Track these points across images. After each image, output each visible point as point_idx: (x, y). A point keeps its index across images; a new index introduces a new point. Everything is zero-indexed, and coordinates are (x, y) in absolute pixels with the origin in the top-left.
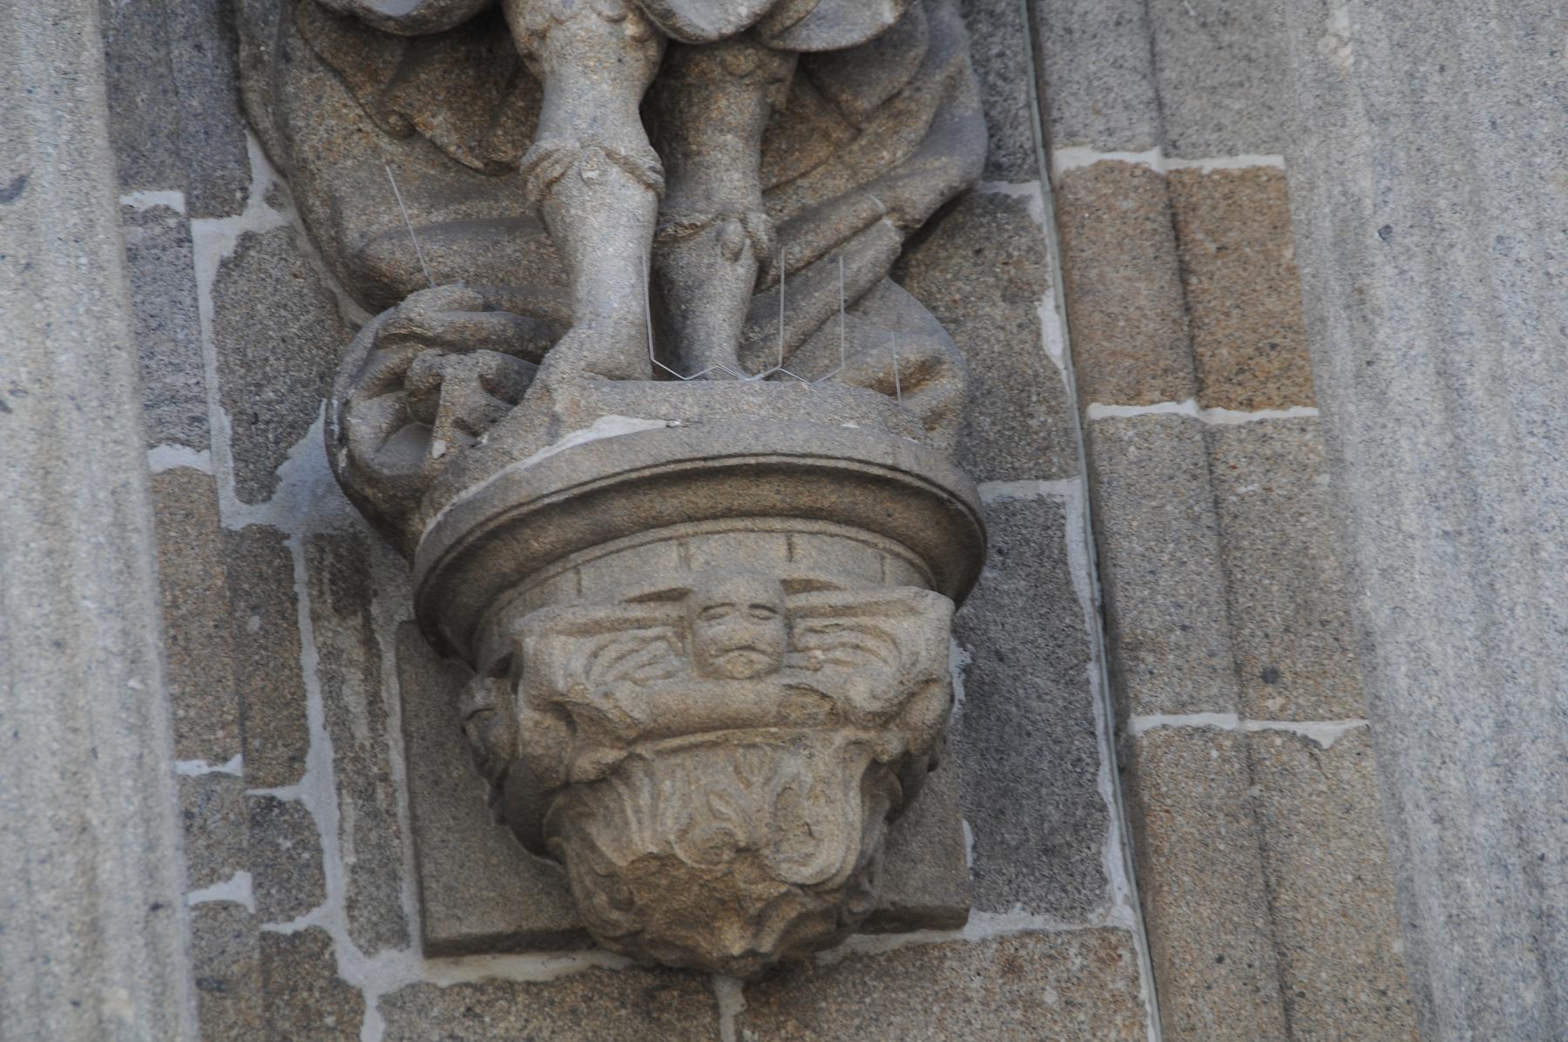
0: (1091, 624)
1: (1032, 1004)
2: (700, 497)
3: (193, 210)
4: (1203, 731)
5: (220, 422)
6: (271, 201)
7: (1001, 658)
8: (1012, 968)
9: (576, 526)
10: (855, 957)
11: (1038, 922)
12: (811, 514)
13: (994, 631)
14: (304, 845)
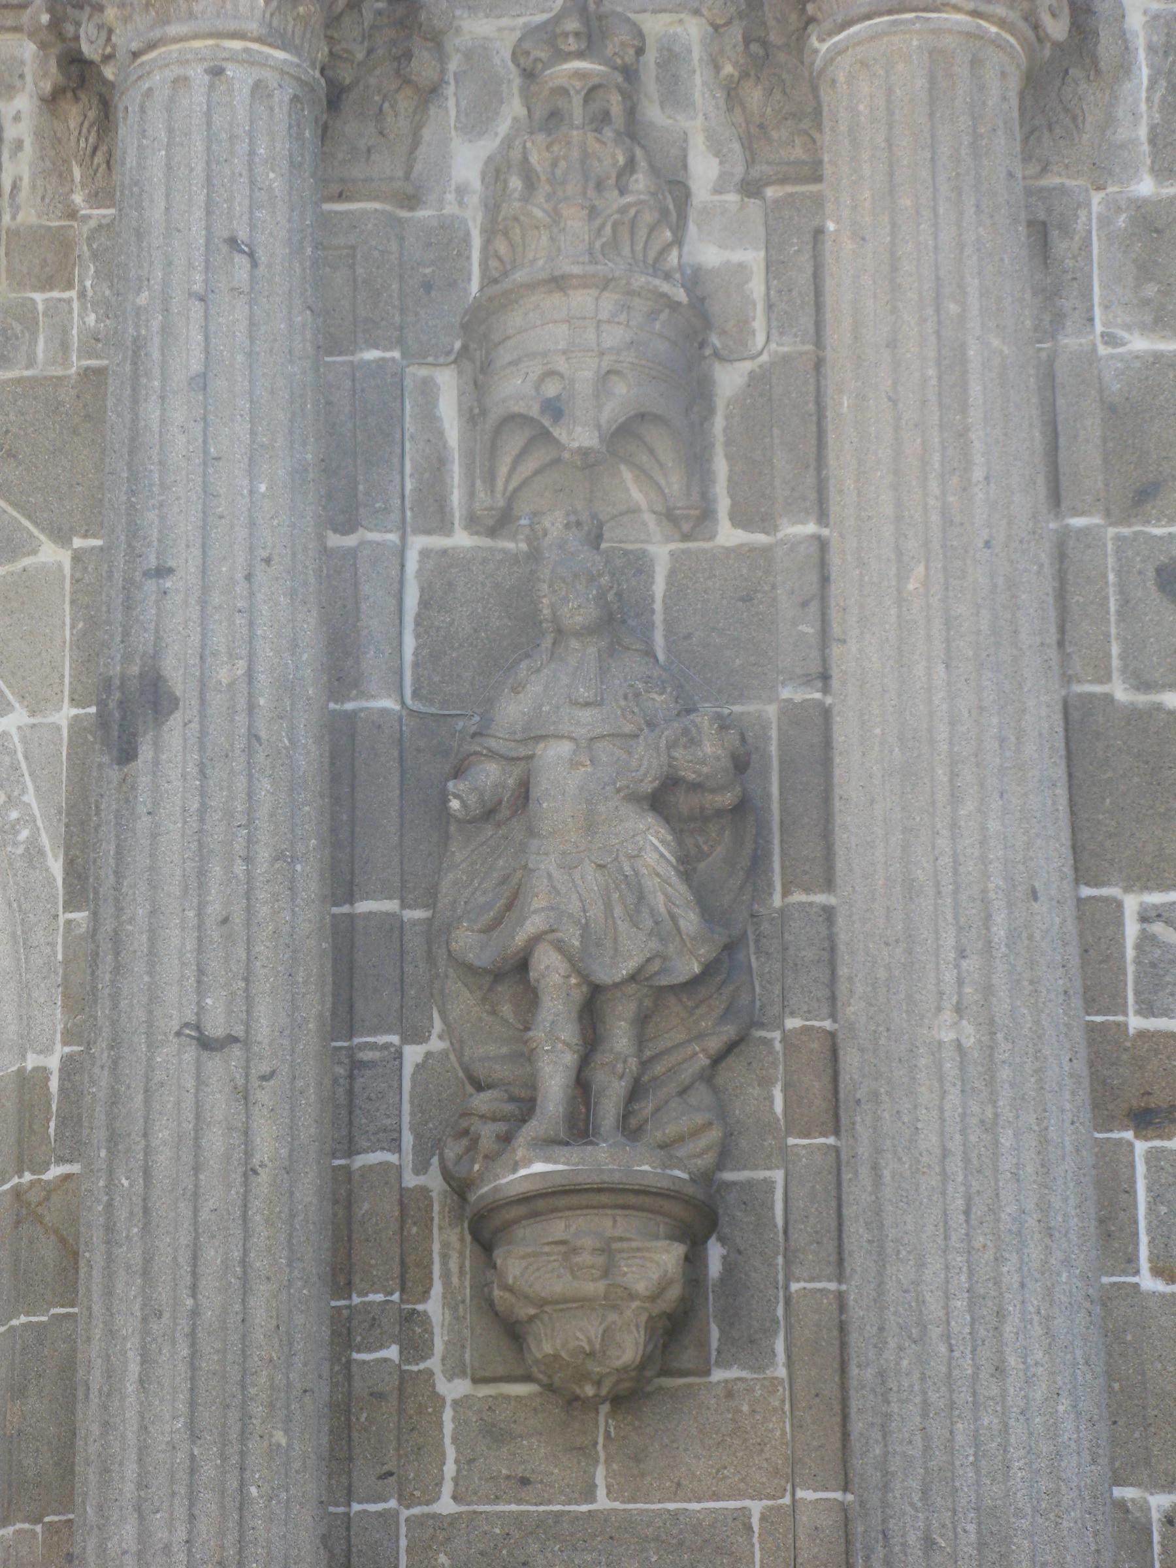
0: (781, 1237)
1: (738, 1411)
2: (574, 1200)
3: (406, 1040)
4: (821, 1290)
5: (408, 1139)
6: (440, 1037)
7: (740, 1252)
8: (730, 1395)
9: (522, 1210)
10: (660, 1388)
11: (744, 1374)
12: (624, 1207)
13: (738, 1240)
14: (426, 1331)
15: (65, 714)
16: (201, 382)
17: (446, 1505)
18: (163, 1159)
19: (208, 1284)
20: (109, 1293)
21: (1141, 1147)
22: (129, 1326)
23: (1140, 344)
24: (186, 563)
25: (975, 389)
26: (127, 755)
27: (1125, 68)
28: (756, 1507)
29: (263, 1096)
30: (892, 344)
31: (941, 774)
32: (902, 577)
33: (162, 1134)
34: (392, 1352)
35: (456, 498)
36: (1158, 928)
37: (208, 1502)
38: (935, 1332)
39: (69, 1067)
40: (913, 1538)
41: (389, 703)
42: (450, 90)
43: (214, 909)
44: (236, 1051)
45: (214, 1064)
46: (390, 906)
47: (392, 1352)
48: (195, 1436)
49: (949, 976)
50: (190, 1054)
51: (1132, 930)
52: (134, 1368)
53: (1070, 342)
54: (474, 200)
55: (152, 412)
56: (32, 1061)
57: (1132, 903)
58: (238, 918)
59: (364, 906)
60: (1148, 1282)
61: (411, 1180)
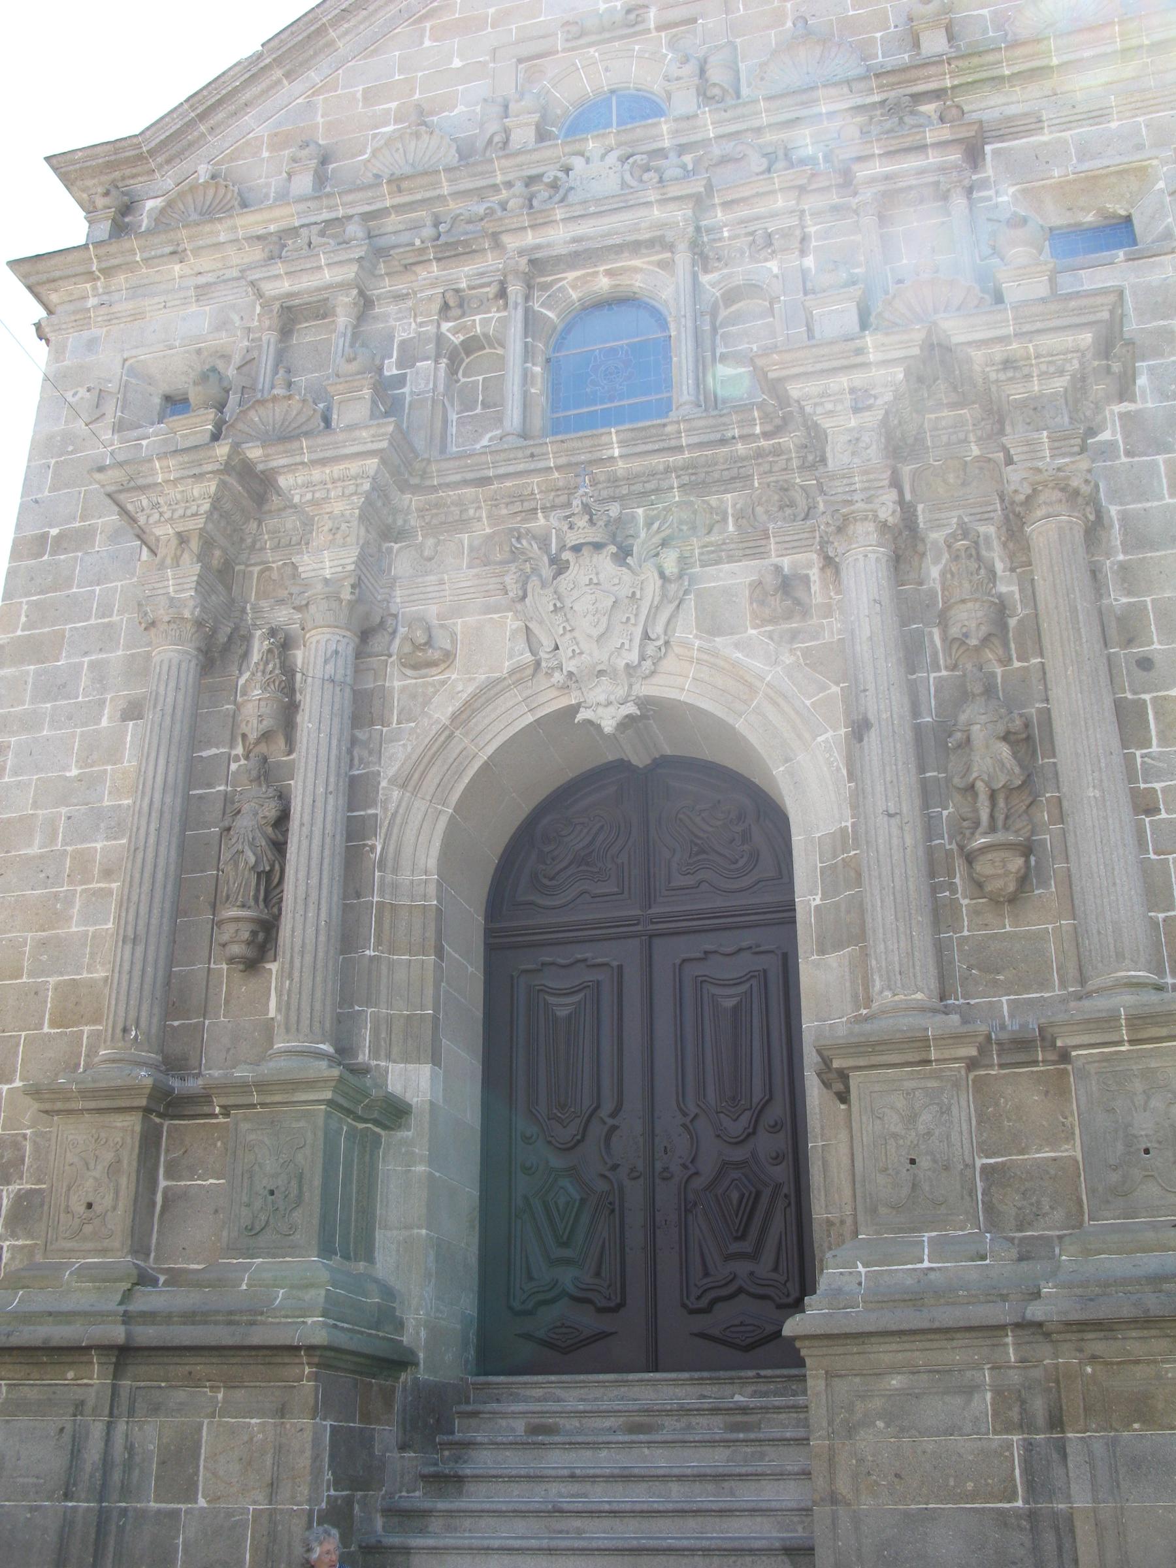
5: (946, 836)
15: (843, 731)
17: (966, 933)
18: (881, 847)
19: (897, 879)
20: (870, 884)
21: (1147, 820)
23: (1124, 600)
24: (871, 687)
25: (1081, 617)
26: (861, 740)
27: (1112, 526)
28: (1050, 927)
29: (906, 828)
30: (1057, 608)
31: (1083, 723)
32: (1066, 671)
34: (947, 893)
35: (942, 662)
36: (1146, 759)
37: (902, 937)
38: (1096, 875)
39: (854, 825)
40: (1095, 932)
43: (888, 779)
45: (893, 821)
46: (935, 774)
48: (897, 920)
49: (1090, 778)
50: (886, 818)
51: (1139, 760)
52: (879, 904)
54: (937, 582)
55: (858, 648)
56: (843, 824)
57: (1138, 753)
59: (928, 775)
60: (1152, 856)
61: (948, 847)
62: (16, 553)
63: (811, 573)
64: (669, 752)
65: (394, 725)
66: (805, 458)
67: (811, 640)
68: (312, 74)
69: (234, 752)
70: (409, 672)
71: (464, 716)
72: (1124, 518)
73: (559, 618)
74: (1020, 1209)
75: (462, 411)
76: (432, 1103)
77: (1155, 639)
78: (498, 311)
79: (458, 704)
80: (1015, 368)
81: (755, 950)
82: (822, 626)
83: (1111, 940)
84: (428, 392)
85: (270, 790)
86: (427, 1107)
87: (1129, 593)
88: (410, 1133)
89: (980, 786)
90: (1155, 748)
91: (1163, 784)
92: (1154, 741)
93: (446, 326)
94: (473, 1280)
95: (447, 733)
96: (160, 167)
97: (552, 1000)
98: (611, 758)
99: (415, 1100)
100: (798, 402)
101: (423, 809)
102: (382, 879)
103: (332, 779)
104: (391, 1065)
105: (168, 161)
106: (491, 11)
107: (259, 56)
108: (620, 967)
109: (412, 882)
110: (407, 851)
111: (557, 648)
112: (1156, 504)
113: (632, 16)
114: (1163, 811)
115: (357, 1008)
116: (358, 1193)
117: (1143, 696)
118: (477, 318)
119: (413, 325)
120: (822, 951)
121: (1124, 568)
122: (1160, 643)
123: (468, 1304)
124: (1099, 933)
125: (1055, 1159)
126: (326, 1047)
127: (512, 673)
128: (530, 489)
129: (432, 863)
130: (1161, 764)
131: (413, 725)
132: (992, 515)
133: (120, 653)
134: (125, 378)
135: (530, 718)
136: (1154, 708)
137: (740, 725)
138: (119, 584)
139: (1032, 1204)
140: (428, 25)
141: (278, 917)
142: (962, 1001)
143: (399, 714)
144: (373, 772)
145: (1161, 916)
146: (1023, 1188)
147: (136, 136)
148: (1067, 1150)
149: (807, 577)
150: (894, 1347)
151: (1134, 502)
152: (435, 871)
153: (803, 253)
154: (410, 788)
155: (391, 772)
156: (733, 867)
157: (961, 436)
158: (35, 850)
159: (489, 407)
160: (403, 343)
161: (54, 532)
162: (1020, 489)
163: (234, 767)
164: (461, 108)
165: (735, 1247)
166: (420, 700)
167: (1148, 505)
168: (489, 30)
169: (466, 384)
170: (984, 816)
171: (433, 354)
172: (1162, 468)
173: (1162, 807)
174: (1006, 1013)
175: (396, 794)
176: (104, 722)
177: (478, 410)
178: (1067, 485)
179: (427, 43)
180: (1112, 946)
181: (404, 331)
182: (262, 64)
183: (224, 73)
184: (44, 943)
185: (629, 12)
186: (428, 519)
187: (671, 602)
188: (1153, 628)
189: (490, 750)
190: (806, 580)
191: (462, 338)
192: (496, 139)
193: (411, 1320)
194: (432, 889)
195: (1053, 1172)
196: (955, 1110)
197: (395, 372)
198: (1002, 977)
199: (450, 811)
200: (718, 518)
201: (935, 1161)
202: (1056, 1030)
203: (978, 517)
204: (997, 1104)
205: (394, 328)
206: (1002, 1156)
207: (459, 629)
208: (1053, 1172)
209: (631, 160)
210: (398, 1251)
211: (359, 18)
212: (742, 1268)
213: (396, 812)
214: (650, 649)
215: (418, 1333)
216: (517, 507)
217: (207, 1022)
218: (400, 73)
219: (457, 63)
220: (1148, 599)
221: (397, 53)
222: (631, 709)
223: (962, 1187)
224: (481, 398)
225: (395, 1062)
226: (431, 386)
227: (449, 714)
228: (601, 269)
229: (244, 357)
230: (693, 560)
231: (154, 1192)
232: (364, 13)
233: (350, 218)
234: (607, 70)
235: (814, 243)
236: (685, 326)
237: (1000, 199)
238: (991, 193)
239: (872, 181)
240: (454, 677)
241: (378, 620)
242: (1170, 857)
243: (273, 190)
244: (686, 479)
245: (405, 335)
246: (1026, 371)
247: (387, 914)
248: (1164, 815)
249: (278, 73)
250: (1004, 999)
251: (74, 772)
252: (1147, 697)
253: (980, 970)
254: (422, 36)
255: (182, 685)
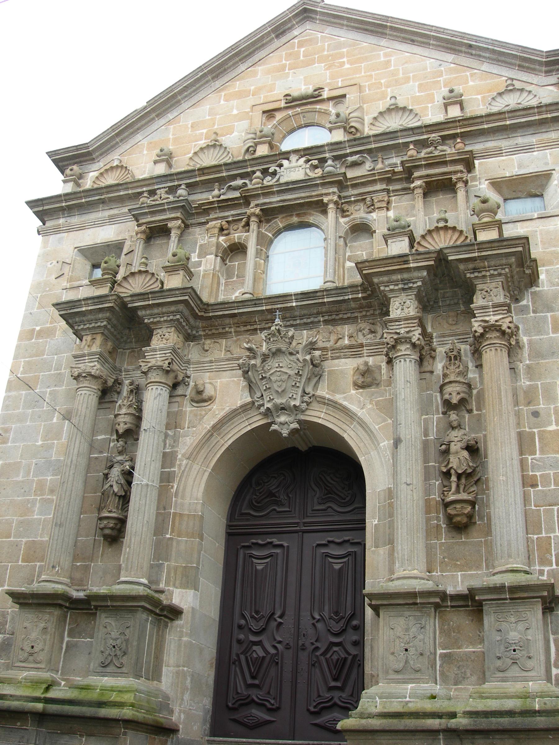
5: (437, 494)
16: (404, 399)
17: (443, 541)
18: (403, 500)
19: (409, 515)
21: (532, 490)
22: (399, 521)
23: (528, 383)
24: (403, 422)
25: (502, 393)
26: (397, 448)
27: (524, 346)
28: (483, 540)
29: (414, 491)
30: (491, 388)
32: (494, 419)
33: (402, 497)
35: (440, 410)
40: (499, 544)
41: (432, 437)
42: (437, 357)
43: (408, 467)
44: (411, 486)
45: (408, 487)
46: (434, 464)
47: (436, 522)
48: (407, 535)
49: (501, 471)
50: (405, 485)
51: (530, 461)
53: (518, 384)
55: (398, 404)
56: (390, 486)
57: (530, 458)
58: (411, 468)
59: (430, 464)
60: (533, 508)
61: (437, 499)
62: (20, 338)
63: (382, 364)
64: (316, 444)
65: (186, 429)
66: (382, 310)
67: (380, 397)
68: (169, 115)
69: (112, 438)
70: (195, 404)
71: (218, 426)
72: (530, 342)
73: (264, 382)
74: (456, 674)
75: (227, 279)
76: (193, 608)
77: (541, 402)
78: (246, 232)
79: (216, 420)
80: (479, 272)
81: (351, 541)
82: (385, 390)
83: (506, 549)
84: (211, 270)
85: (127, 457)
86: (190, 610)
87: (531, 380)
88: (182, 622)
89: (452, 471)
90: (538, 456)
91: (541, 473)
92: (538, 452)
93: (222, 238)
94: (210, 691)
95: (210, 433)
96: (97, 157)
97: (255, 561)
98: (289, 446)
99: (185, 606)
100: (377, 284)
101: (197, 469)
102: (176, 501)
103: (154, 455)
104: (175, 589)
105: (101, 155)
106: (252, 88)
107: (145, 108)
108: (288, 547)
109: (190, 503)
110: (188, 489)
111: (262, 396)
112: (546, 337)
113: (317, 92)
114: (540, 486)
115: (160, 562)
116: (155, 649)
117: (534, 430)
118: (236, 235)
119: (206, 237)
120: (377, 546)
121: (529, 367)
122: (543, 404)
123: (207, 702)
124: (501, 545)
125: (474, 652)
126: (144, 581)
127: (241, 407)
128: (254, 319)
129: (200, 495)
130: (540, 463)
131: (194, 429)
132: (468, 339)
133: (64, 387)
134: (74, 257)
135: (249, 428)
136: (538, 436)
137: (345, 436)
138: (66, 355)
139: (462, 673)
140: (223, 94)
141: (126, 517)
142: (439, 573)
143: (189, 423)
144: (175, 451)
145: (536, 536)
146: (458, 665)
147: (87, 144)
148: (480, 648)
149: (380, 366)
150: (388, 737)
151: (535, 335)
152: (201, 499)
153: (388, 209)
154: (191, 459)
155: (183, 451)
156: (343, 501)
157: (456, 301)
158: (20, 478)
159: (240, 277)
160: (201, 245)
161: (38, 328)
162: (478, 330)
163: (112, 444)
164: (235, 134)
165: (333, 684)
166: (199, 417)
167: (542, 337)
168: (251, 96)
169: (230, 266)
170: (454, 486)
171: (214, 252)
172: (550, 319)
173: (539, 484)
174: (460, 580)
175: (185, 462)
176: (55, 420)
177: (235, 279)
178: (501, 329)
179: (222, 102)
180: (506, 552)
181: (202, 240)
182: (146, 111)
183: (128, 116)
184: (22, 522)
185: (315, 90)
186: (207, 331)
187: (316, 376)
188: (540, 397)
189: (230, 442)
190: (380, 368)
191: (228, 244)
192: (251, 149)
193: (177, 709)
194: (199, 507)
195: (473, 658)
196: (428, 627)
197: (197, 259)
198: (459, 563)
199: (210, 470)
200: (341, 336)
201: (416, 650)
202: (476, 592)
203: (462, 340)
204: (449, 624)
205: (197, 239)
206: (450, 649)
207: (218, 385)
208: (473, 658)
209: (310, 163)
210: (173, 677)
211: (192, 90)
212: (336, 694)
213: (184, 470)
214: (306, 398)
215: (180, 716)
216: (249, 327)
217: (92, 564)
218: (209, 116)
219: (235, 112)
220: (539, 383)
221: (208, 107)
222: (295, 425)
223: (428, 663)
224: (236, 273)
225: (177, 588)
226: (213, 267)
227: (211, 425)
228: (295, 213)
229: (128, 249)
230: (327, 356)
231: (62, 643)
232: (194, 88)
233: (180, 185)
234: (304, 117)
235: (393, 205)
236: (330, 244)
237: (481, 187)
238: (477, 183)
239: (420, 178)
240: (214, 407)
241: (181, 379)
242: (542, 508)
243: (147, 169)
244: (326, 318)
245: (202, 242)
246: (484, 273)
247: (177, 518)
248: (540, 488)
249: (154, 115)
250: (459, 573)
251: (40, 443)
252: (535, 430)
253: (449, 559)
254: (220, 98)
255: (89, 406)
